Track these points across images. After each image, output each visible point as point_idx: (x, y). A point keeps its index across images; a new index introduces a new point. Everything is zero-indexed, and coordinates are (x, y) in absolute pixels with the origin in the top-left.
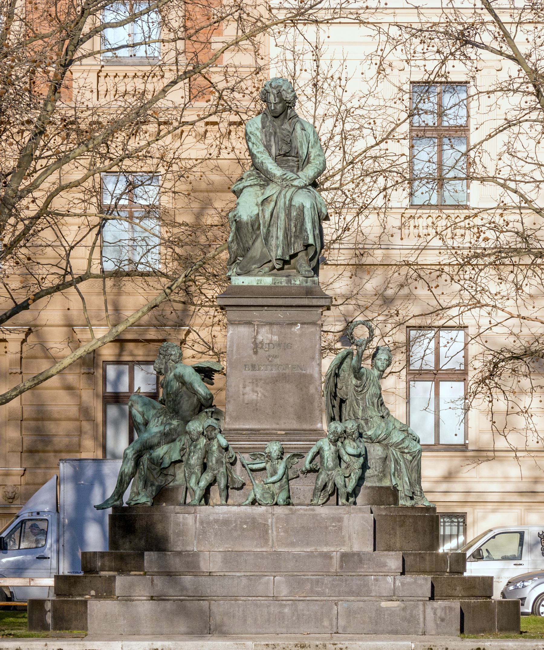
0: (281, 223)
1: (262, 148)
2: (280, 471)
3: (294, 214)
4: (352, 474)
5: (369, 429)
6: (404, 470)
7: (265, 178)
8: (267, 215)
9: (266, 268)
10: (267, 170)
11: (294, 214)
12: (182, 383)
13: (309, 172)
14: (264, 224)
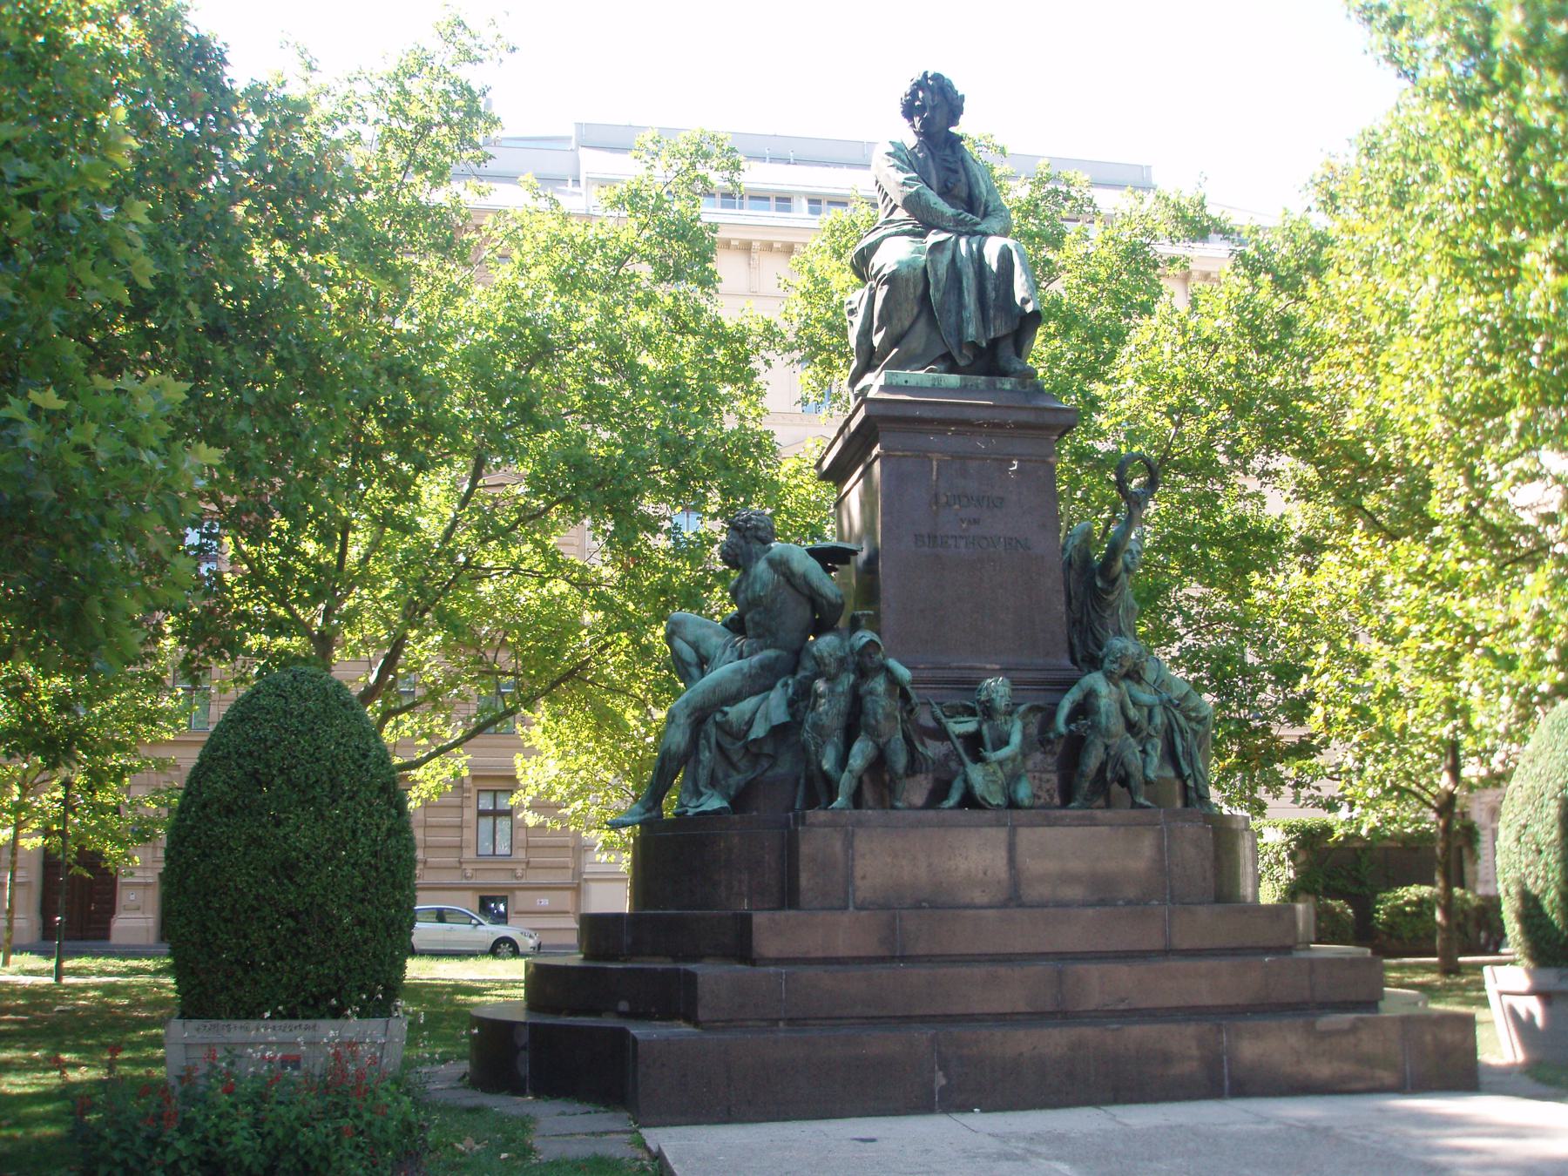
0: (969, 282)
2: (1016, 738)
4: (1149, 747)
12: (784, 575)
14: (937, 282)
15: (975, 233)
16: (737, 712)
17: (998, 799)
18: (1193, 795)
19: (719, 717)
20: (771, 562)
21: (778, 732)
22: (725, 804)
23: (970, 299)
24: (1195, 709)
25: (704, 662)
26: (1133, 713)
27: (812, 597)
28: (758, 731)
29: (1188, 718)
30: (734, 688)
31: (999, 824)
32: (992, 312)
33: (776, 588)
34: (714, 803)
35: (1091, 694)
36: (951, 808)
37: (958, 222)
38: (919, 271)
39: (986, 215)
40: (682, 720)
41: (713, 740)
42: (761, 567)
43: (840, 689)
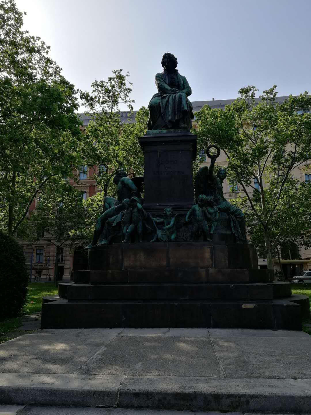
2: (172, 223)
3: (177, 100)
5: (219, 205)
8: (164, 103)
10: (164, 88)
11: (177, 100)
14: (163, 107)
15: (176, 93)
19: (107, 221)
21: (119, 224)
22: (106, 243)
24: (238, 215)
25: (110, 207)
26: (208, 215)
28: (114, 224)
29: (237, 218)
32: (177, 113)
35: (194, 210)
36: (153, 242)
38: (157, 104)
39: (184, 89)
40: (99, 222)
41: (106, 227)
42: (120, 183)
43: (128, 212)
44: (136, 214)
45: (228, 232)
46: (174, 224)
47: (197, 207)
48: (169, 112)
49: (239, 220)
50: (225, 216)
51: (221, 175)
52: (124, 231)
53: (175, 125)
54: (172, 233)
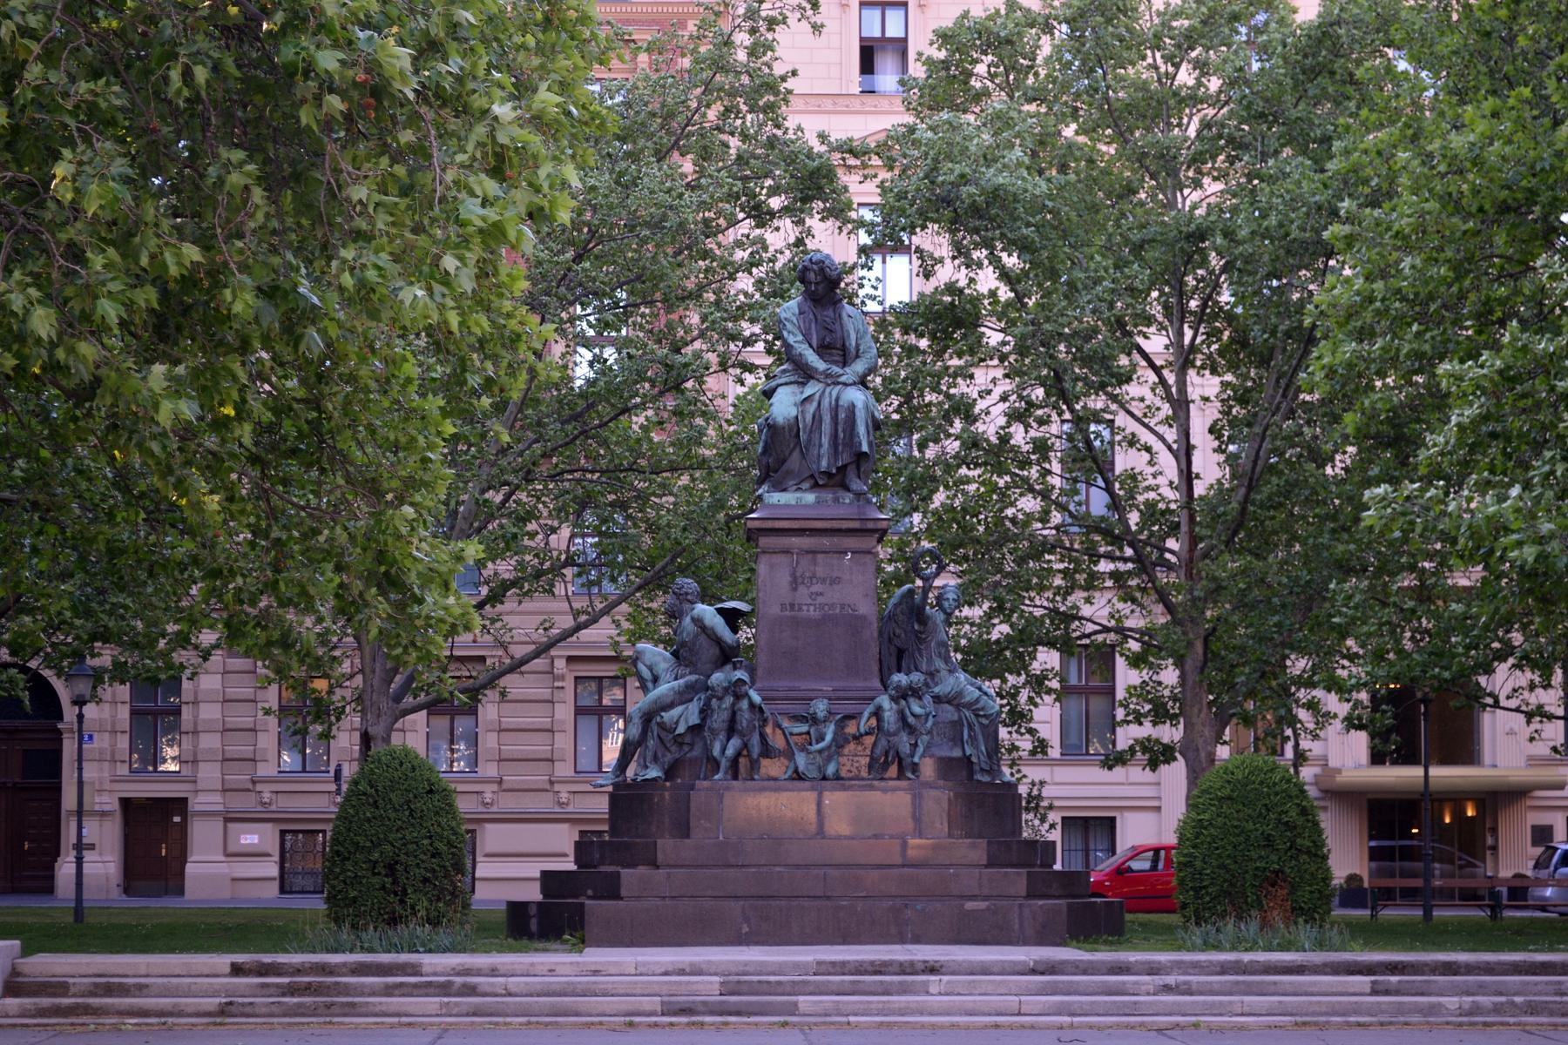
0: (826, 426)
1: (800, 338)
2: (829, 737)
3: (842, 415)
6: (980, 737)
7: (805, 374)
8: (809, 417)
9: (806, 485)
13: (859, 367)
16: (668, 716)
17: (814, 774)
18: (977, 768)
20: (693, 619)
21: (695, 730)
23: (825, 440)
25: (656, 680)
26: (911, 720)
27: (718, 641)
28: (681, 729)
29: (977, 716)
30: (669, 700)
31: (813, 789)
33: (696, 636)
34: (654, 773)
37: (828, 376)
39: (857, 356)
42: (688, 620)
44: (747, 715)
45: (957, 753)
46: (834, 739)
47: (885, 701)
48: (821, 446)
49: (985, 721)
50: (949, 713)
51: (946, 604)
52: (716, 752)
53: (835, 480)
54: (829, 759)
